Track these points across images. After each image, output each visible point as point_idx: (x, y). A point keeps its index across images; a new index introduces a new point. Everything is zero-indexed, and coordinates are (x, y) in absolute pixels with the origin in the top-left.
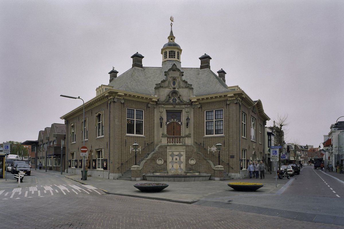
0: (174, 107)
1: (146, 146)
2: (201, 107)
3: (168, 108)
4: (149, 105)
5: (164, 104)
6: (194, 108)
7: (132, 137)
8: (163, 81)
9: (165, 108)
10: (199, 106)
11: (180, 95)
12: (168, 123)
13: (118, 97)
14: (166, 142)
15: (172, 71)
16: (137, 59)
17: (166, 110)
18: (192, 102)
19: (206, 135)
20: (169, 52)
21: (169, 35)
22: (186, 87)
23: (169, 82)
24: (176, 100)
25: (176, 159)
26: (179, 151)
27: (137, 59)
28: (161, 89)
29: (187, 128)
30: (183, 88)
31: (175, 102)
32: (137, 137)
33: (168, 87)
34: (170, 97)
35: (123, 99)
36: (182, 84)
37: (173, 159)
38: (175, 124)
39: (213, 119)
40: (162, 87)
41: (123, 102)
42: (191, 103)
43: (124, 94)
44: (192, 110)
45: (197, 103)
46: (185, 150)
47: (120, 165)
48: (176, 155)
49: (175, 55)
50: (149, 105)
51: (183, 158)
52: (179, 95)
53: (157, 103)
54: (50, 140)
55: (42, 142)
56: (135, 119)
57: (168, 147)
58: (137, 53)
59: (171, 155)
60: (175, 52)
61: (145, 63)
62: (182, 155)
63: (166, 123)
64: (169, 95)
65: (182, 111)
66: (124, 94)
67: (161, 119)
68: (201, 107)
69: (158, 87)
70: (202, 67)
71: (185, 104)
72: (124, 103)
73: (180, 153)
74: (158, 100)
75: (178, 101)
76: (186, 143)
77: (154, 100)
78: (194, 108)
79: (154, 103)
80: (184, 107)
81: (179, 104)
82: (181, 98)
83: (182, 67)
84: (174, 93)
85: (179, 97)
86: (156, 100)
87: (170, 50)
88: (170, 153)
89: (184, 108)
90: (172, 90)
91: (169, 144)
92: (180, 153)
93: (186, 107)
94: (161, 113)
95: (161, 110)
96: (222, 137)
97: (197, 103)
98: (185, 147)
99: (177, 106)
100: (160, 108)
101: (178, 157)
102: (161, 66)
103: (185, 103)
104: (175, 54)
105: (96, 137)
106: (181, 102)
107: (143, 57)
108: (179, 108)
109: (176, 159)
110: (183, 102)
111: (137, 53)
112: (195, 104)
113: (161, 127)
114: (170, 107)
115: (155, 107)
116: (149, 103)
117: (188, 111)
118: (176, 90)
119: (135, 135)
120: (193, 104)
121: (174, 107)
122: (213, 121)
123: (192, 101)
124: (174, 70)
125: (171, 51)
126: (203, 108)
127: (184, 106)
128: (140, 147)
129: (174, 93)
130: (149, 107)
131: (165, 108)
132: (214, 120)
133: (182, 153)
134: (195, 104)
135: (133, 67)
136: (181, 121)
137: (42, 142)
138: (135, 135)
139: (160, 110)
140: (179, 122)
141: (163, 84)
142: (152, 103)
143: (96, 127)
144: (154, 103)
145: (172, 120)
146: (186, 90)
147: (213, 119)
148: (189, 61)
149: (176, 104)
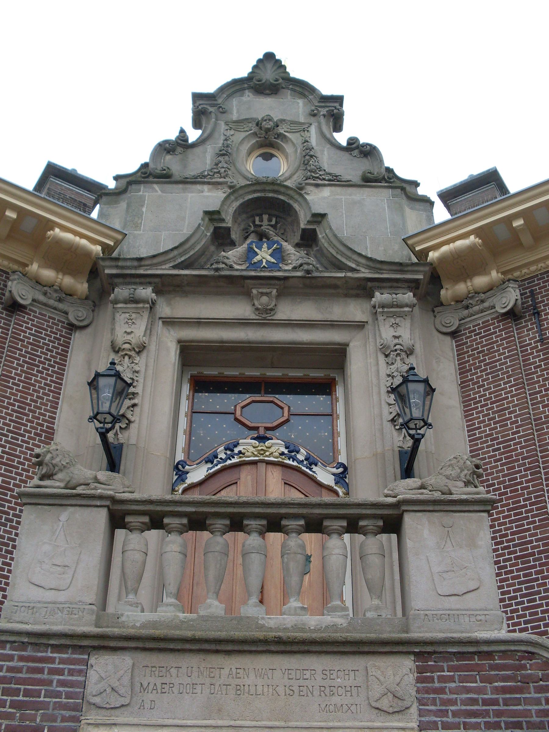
0: (265, 318)
3: (199, 323)
6: (454, 334)
8: (177, 146)
9: (169, 322)
10: (511, 297)
18: (435, 279)
42: (426, 283)
45: (480, 281)
64: (212, 216)
65: (337, 356)
71: (363, 289)
76: (421, 597)
79: (68, 281)
81: (309, 286)
85: (308, 239)
89: (360, 326)
97: (480, 281)
98: (400, 671)
100: (121, 318)
103: (365, 273)
110: (353, 270)
112: (461, 288)
114: (223, 317)
115: (76, 314)
120: (446, 293)
123: (433, 255)
127: (355, 310)
131: (169, 322)
136: (335, 458)
139: (120, 329)
140: (311, 462)
141: (172, 163)
142: (48, 274)
144: (68, 281)
146: (377, 199)
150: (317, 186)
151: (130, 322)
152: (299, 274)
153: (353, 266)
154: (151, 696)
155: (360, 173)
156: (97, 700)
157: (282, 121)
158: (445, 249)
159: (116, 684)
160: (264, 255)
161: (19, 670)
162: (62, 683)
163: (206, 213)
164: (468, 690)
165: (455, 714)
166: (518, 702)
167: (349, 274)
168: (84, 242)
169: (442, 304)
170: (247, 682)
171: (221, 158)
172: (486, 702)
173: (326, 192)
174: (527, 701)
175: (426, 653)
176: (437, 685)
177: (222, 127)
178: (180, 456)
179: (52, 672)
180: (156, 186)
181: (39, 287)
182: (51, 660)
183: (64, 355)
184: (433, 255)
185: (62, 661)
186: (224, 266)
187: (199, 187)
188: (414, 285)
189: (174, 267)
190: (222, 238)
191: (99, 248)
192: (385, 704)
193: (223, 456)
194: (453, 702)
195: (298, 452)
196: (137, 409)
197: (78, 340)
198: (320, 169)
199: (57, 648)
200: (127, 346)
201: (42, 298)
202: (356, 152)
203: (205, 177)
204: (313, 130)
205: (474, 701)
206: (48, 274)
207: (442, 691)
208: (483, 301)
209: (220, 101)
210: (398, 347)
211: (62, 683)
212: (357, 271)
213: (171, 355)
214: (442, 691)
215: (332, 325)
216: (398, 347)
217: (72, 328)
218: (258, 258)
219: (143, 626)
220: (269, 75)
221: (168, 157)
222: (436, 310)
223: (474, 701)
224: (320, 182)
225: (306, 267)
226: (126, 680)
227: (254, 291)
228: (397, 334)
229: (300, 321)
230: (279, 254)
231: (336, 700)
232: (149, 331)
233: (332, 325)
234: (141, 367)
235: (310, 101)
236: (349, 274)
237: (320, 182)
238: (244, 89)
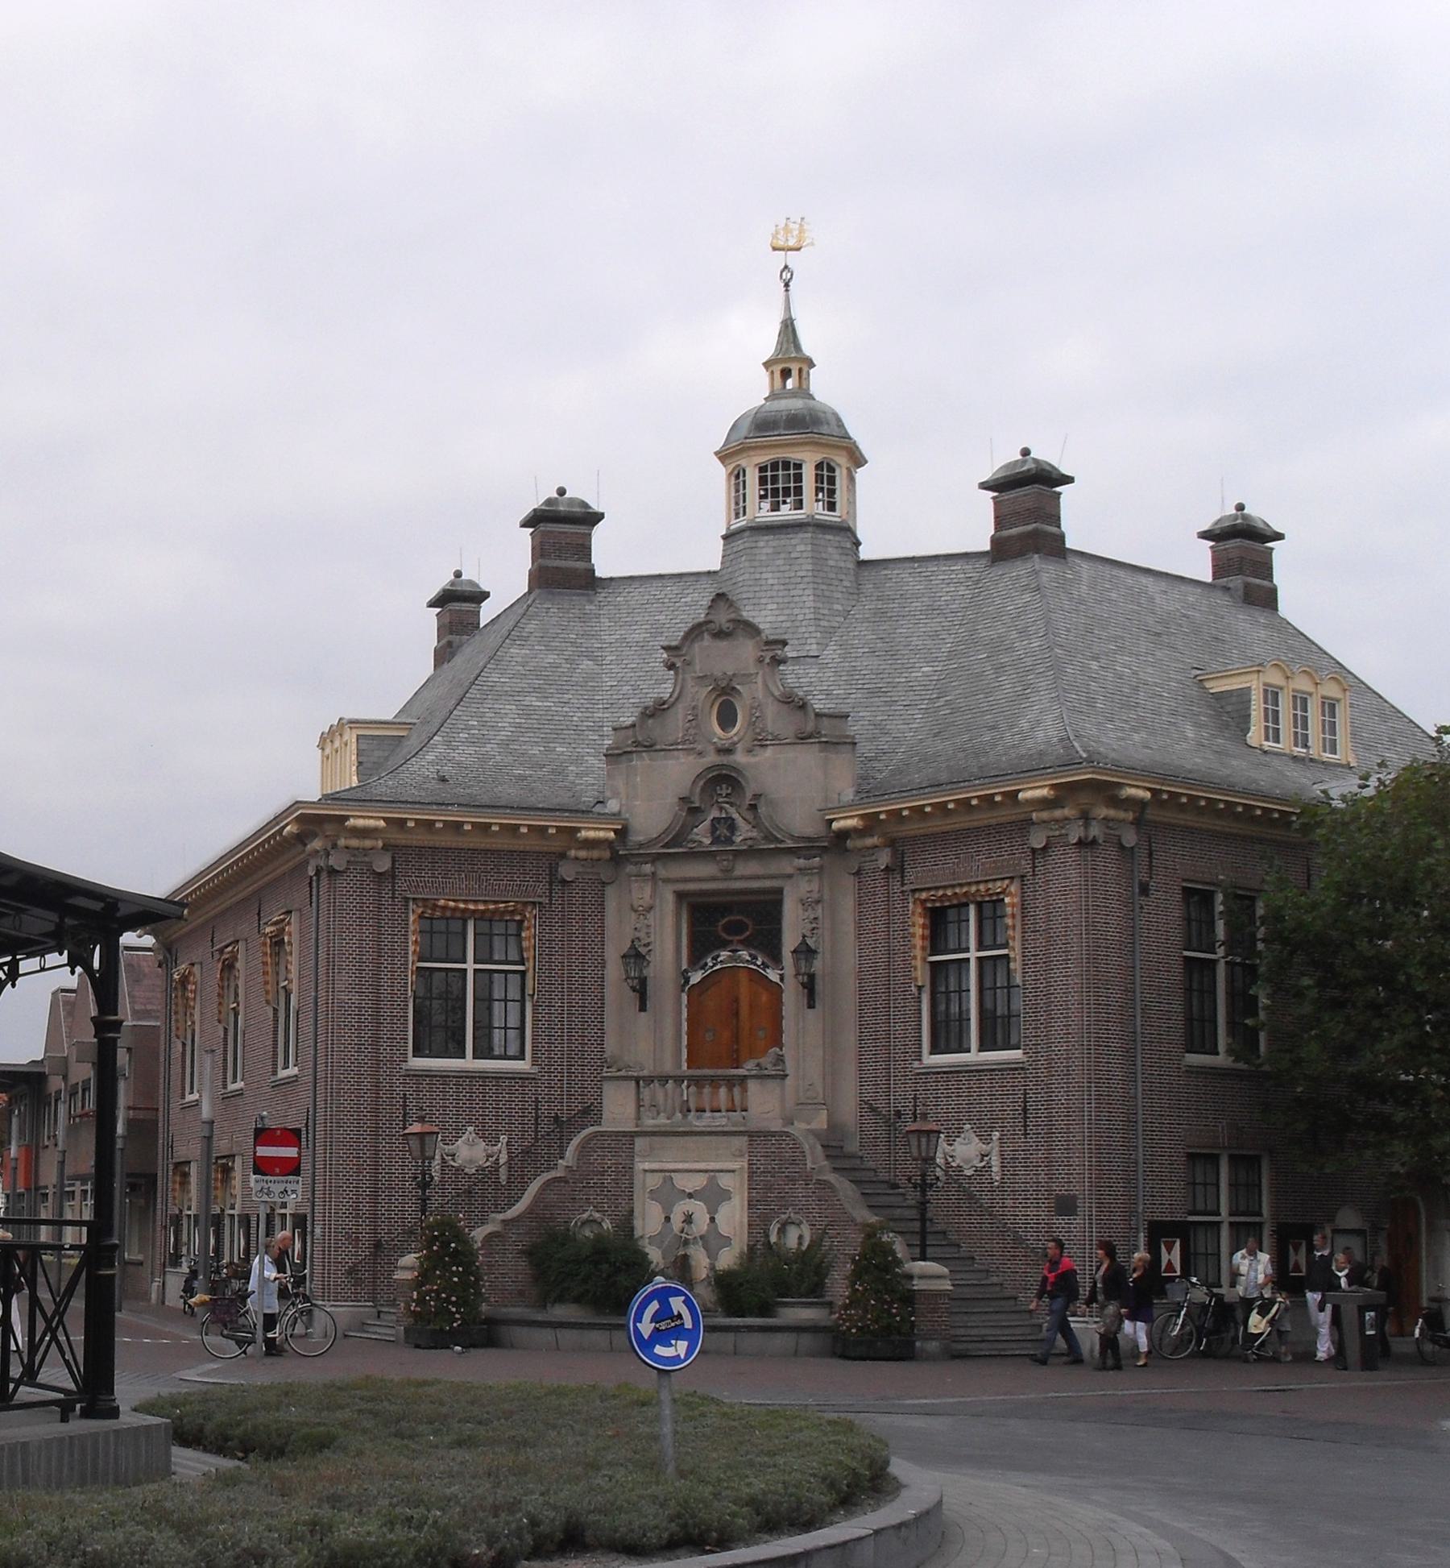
1: (544, 1128)
2: (896, 869)
4: (566, 871)
5: (656, 858)
6: (858, 873)
7: (444, 1077)
8: (657, 710)
9: (667, 881)
10: (884, 859)
12: (696, 977)
13: (354, 843)
14: (631, 1109)
15: (707, 640)
16: (562, 529)
17: (680, 896)
18: (844, 834)
19: (935, 1049)
20: (763, 469)
21: (767, 343)
22: (803, 738)
23: (695, 718)
24: (732, 826)
25: (688, 1219)
26: (706, 1171)
27: (562, 529)
28: (641, 762)
29: (811, 1006)
30: (778, 741)
31: (731, 842)
32: (483, 1077)
33: (688, 745)
34: (694, 811)
35: (385, 847)
36: (775, 719)
37: (668, 1219)
38: (743, 978)
39: (967, 950)
40: (650, 747)
41: (383, 864)
43: (384, 819)
44: (849, 882)
46: (741, 1164)
47: (364, 1252)
48: (690, 1196)
49: (799, 491)
50: (566, 871)
52: (749, 795)
53: (620, 852)
54: (72, 1080)
55: (65, 1078)
56: (470, 966)
57: (640, 1143)
58: (562, 492)
59: (654, 1194)
60: (799, 466)
61: (609, 555)
62: (725, 1195)
63: (687, 980)
66: (384, 819)
67: (636, 956)
68: (896, 869)
69: (636, 743)
70: (1002, 550)
71: (790, 851)
72: (392, 875)
73: (712, 1182)
74: (622, 833)
75: (744, 832)
77: (592, 834)
78: (858, 873)
79: (595, 854)
80: (789, 870)
81: (751, 853)
82: (762, 810)
83: (865, 553)
84: (723, 780)
85: (753, 807)
86: (602, 834)
87: (765, 458)
88: (654, 1181)
89: (790, 876)
90: (712, 758)
91: (649, 1123)
92: (712, 1182)
93: (801, 870)
94: (647, 919)
95: (642, 893)
96: (1013, 1068)
99: (744, 868)
100: (635, 886)
101: (698, 1208)
102: (716, 566)
103: (790, 844)
104: (798, 478)
105: (275, 1073)
106: (769, 837)
107: (598, 517)
108: (758, 877)
109: (688, 1219)
110: (782, 841)
111: (562, 492)
112: (859, 843)
113: (643, 1008)
114: (702, 875)
116: (563, 856)
117: (816, 896)
118: (740, 758)
119: (469, 1063)
121: (727, 874)
122: (968, 960)
123: (835, 825)
124: (720, 635)
125: (775, 466)
126: (911, 875)
127: (788, 865)
128: (504, 1139)
129: (723, 780)
130: (564, 882)
131: (667, 881)
132: (973, 955)
133: (725, 1181)
135: (530, 592)
137: (65, 1078)
138: (469, 1063)
140: (765, 966)
142: (582, 854)
143: (275, 1010)
144: (595, 854)
145: (724, 954)
146: (808, 758)
147: (967, 950)
148: (918, 504)
149: (737, 854)
160: (723, 831)
173: (769, 752)
175: (751, 1135)
177: (690, 683)
178: (684, 967)
183: (602, 904)
184: (835, 825)
189: (665, 846)
191: (612, 834)
197: (610, 891)
198: (763, 730)
206: (582, 854)
212: (782, 841)
213: (670, 898)
215: (772, 877)
217: (604, 884)
220: (722, 618)
221: (650, 721)
229: (749, 875)
232: (654, 891)
233: (772, 877)
234: (651, 922)
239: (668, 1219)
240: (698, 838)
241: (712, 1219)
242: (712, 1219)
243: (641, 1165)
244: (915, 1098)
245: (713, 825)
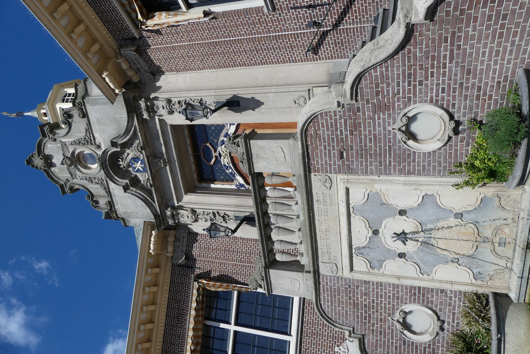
11: (114, 144)
22: (84, 115)
25: (402, 236)
30: (89, 129)
37: (402, 255)
45: (124, 66)
48: (376, 232)
51: (400, 191)
64: (126, 188)
79: (171, 239)
84: (112, 164)
98: (316, 180)
114: (171, 177)
134: (130, 73)
144: (171, 239)
150: (94, 139)
151: (183, 216)
152: (144, 152)
153: (133, 128)
154: (332, 257)
155: (81, 119)
156: (335, 273)
157: (64, 155)
158: (112, 86)
159: (329, 268)
161: (328, 294)
162: (331, 282)
163: (125, 192)
164: (321, 156)
165: (330, 161)
166: (324, 138)
167: (138, 130)
168: (152, 239)
169: (140, 80)
170: (324, 228)
171: (94, 182)
172: (325, 149)
174: (324, 134)
175: (307, 169)
176: (320, 166)
179: (327, 285)
180: (116, 207)
181: (176, 250)
182: (323, 285)
185: (324, 293)
186: (148, 183)
187: (111, 190)
188: (136, 100)
189: (154, 202)
190: (135, 182)
191: (153, 232)
192: (328, 185)
193: (230, 170)
194: (326, 161)
195: (223, 140)
196: (220, 212)
199: (319, 284)
200: (193, 217)
201: (180, 248)
202: (70, 120)
203: (105, 188)
204: (64, 140)
205: (325, 153)
206: (170, 248)
207: (322, 164)
208: (134, 63)
209: (62, 183)
210: (168, 107)
211: (331, 282)
212: (135, 127)
214: (322, 164)
216: (168, 107)
218: (140, 168)
219: (308, 257)
222: (143, 83)
223: (325, 153)
224: (92, 138)
225: (140, 150)
226: (327, 265)
227: (157, 168)
228: (162, 108)
230: (135, 159)
231: (328, 201)
235: (46, 141)
236: (138, 130)
237: (92, 138)
238: (51, 172)
239: (402, 255)
240: (146, 182)
241: (402, 213)
242: (402, 213)
243: (347, 274)
244: (295, 8)
245: (137, 171)
